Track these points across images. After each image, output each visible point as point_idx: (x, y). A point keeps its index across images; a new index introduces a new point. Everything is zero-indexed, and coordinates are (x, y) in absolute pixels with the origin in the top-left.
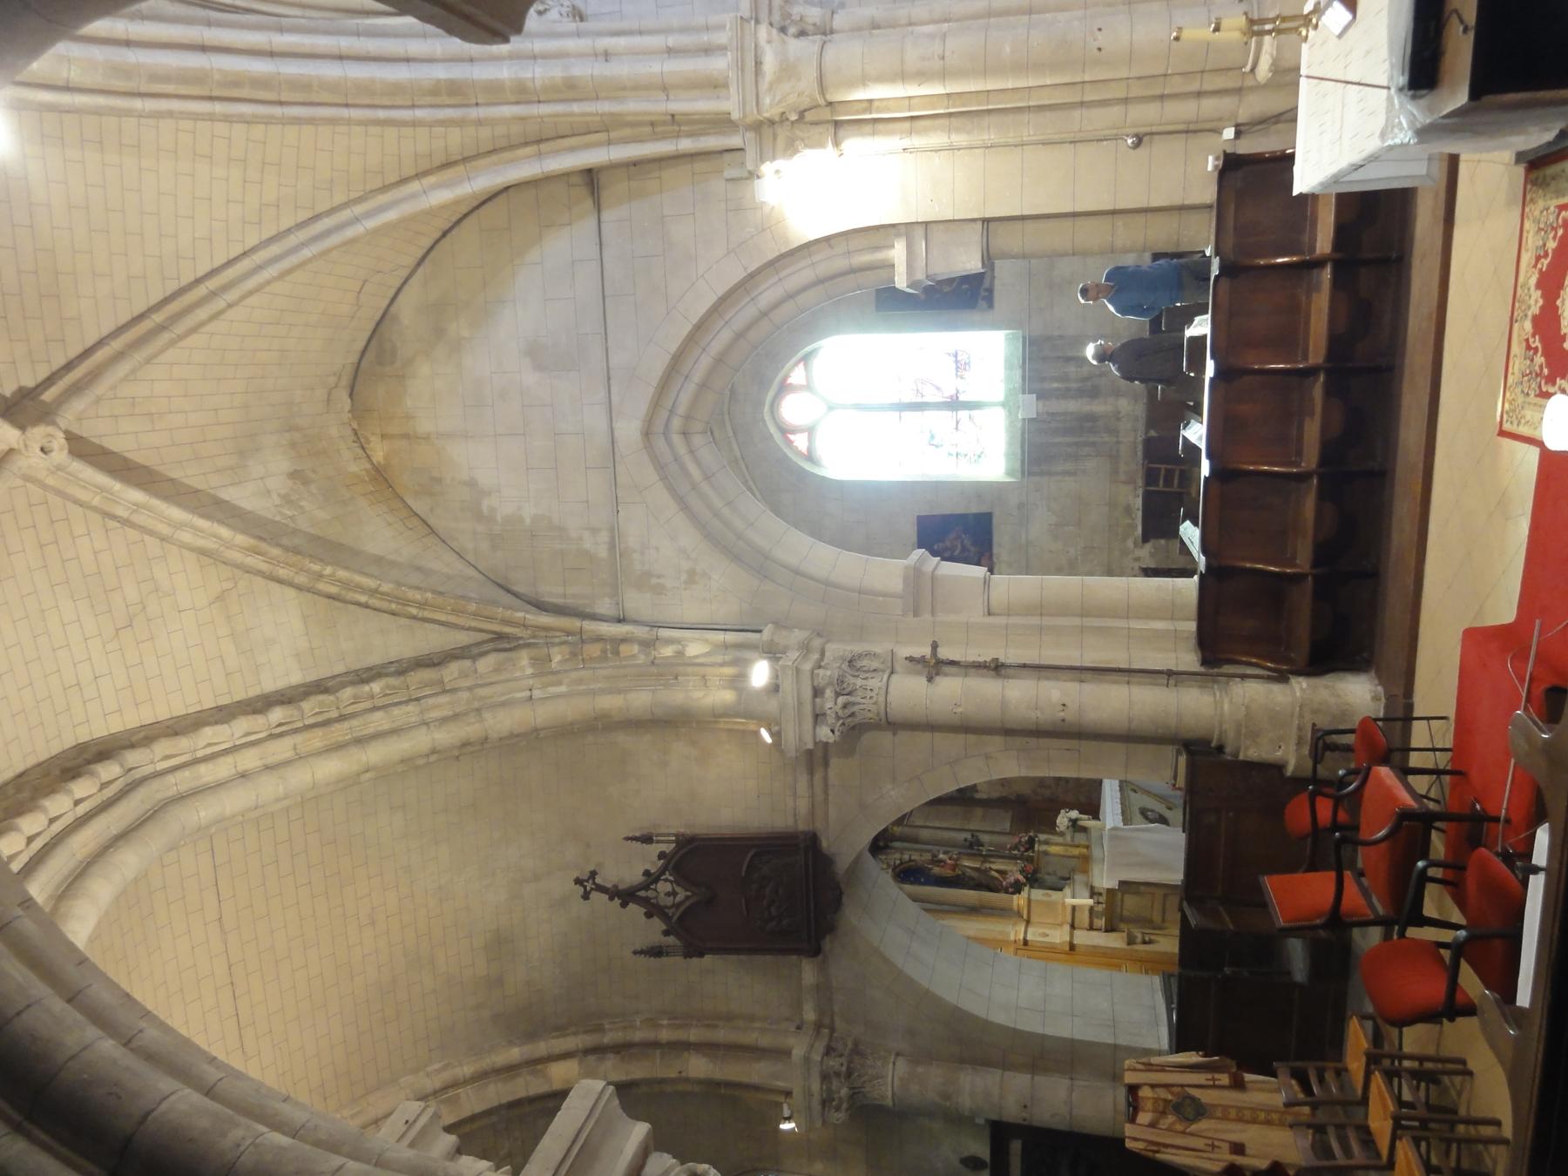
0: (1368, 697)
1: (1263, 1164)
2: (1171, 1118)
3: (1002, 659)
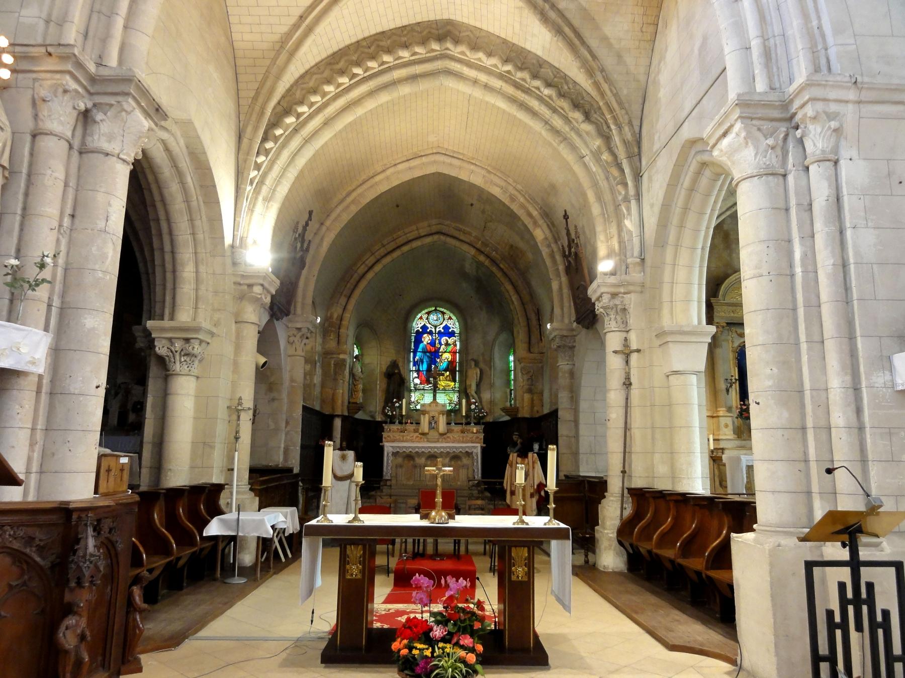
0: (606, 564)
3: (632, 387)
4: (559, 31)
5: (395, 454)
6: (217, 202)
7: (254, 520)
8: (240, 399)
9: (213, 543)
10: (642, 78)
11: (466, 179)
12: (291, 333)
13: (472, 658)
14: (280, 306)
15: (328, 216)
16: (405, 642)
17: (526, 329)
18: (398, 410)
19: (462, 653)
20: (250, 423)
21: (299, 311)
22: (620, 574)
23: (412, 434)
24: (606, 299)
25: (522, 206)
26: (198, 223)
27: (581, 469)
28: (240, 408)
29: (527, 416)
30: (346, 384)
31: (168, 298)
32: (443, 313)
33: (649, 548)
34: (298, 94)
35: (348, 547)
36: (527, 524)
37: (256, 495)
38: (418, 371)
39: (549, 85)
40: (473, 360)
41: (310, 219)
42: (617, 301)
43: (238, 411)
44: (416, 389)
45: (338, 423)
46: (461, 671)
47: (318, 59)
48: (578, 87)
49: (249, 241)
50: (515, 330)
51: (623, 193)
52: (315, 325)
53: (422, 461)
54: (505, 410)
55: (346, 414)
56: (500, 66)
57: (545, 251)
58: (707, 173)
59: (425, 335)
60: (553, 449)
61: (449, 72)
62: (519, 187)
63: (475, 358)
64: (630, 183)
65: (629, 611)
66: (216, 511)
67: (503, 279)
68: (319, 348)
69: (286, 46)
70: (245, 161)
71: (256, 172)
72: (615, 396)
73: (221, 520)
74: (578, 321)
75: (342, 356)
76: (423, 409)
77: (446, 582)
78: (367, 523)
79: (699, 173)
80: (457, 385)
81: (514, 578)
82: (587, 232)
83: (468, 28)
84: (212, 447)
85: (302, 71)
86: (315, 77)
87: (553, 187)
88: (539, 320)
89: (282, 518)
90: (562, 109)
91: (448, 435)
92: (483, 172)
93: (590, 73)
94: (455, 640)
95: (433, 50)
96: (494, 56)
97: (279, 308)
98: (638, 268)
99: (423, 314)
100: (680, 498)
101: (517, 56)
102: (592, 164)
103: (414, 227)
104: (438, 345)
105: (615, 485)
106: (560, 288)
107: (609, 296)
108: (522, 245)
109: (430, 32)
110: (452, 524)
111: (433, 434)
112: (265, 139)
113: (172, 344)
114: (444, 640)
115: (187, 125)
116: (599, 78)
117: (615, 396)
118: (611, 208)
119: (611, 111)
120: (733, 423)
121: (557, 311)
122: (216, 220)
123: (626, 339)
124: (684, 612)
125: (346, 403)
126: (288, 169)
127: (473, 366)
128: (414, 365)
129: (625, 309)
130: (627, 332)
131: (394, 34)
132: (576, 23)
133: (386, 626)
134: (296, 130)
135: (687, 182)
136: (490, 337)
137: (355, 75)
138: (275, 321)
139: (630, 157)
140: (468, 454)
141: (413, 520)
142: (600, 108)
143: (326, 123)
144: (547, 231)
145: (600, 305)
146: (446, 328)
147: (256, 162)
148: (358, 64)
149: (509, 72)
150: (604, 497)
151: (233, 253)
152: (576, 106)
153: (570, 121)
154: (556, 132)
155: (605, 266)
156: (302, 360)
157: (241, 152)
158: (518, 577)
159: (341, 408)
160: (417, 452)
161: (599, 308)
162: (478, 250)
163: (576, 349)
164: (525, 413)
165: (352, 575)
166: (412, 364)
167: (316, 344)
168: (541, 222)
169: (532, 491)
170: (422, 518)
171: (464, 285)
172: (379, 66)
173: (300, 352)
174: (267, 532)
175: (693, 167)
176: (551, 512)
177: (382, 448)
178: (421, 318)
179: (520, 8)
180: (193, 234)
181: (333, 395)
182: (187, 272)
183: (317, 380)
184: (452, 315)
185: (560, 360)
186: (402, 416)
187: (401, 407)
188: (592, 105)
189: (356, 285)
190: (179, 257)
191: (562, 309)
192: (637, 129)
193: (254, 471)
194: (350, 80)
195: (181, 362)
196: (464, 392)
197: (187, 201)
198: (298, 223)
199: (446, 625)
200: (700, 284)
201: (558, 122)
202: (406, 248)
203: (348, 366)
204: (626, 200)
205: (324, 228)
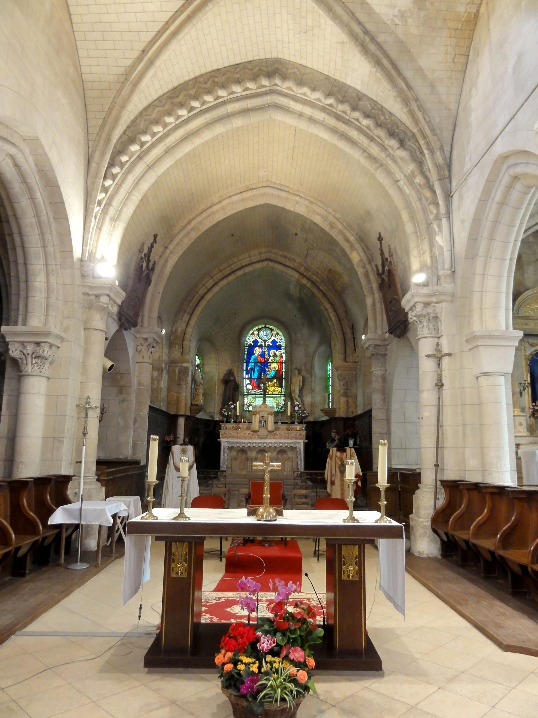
2: (340, 463)
3: (444, 388)
4: (378, 63)
5: (231, 448)
6: (66, 219)
7: (95, 510)
8: (88, 398)
9: (56, 531)
10: (453, 107)
11: (291, 209)
13: (302, 676)
14: (128, 317)
15: (172, 241)
16: (230, 654)
18: (233, 411)
19: (293, 670)
20: (97, 420)
21: (146, 323)
22: (435, 559)
24: (419, 308)
25: (341, 233)
26: (48, 237)
28: (87, 406)
30: (189, 388)
31: (21, 306)
32: (272, 330)
33: (466, 537)
34: (142, 125)
35: (173, 544)
36: (358, 521)
37: (102, 485)
38: (250, 378)
39: (367, 116)
40: (295, 368)
41: (155, 241)
42: (430, 310)
43: (86, 409)
44: (249, 394)
45: (181, 422)
46: (292, 691)
47: (160, 93)
48: (393, 118)
49: (98, 256)
50: (333, 344)
51: (435, 212)
52: (160, 336)
54: (325, 411)
55: (188, 413)
56: (323, 99)
57: (360, 272)
58: (519, 186)
59: (256, 348)
60: (385, 444)
61: (277, 107)
62: (338, 215)
63: (298, 367)
64: (441, 203)
65: (451, 601)
66: (63, 500)
67: (323, 300)
68: (165, 358)
69: (130, 79)
70: (94, 183)
71: (103, 195)
72: (428, 396)
73: (66, 510)
74: (391, 331)
75: (185, 365)
76: (255, 410)
77: (274, 584)
78: (193, 520)
79: (510, 187)
80: (283, 390)
81: (344, 577)
82: (399, 252)
83: (294, 65)
84: (61, 442)
85: (145, 104)
86: (157, 109)
87: (368, 213)
89: (124, 506)
90: (379, 138)
91: (276, 432)
92: (307, 203)
93: (406, 102)
94: (284, 653)
95: (263, 86)
96: (318, 90)
97: (127, 319)
98: (449, 280)
99: (254, 330)
100: (495, 490)
101: (338, 91)
102: (405, 188)
104: (267, 357)
105: (428, 478)
106: (374, 304)
107: (422, 305)
108: (339, 268)
109: (260, 70)
110: (280, 521)
111: (263, 431)
112: (111, 165)
113: (25, 347)
114: (273, 653)
115: (34, 142)
116: (414, 107)
117: (428, 396)
118: (423, 226)
119: (424, 137)
120: (527, 421)
121: (371, 323)
122: (65, 235)
123: (438, 344)
124: (507, 605)
125: (189, 405)
126: (133, 192)
127: (297, 374)
128: (247, 373)
129: (436, 317)
130: (439, 338)
131: (227, 71)
132: (393, 55)
133: (215, 620)
134: (140, 158)
135: (498, 196)
137: (192, 108)
138: (124, 331)
139: (441, 179)
140: (293, 449)
141: (238, 516)
142: (414, 135)
143: (168, 151)
144: (362, 254)
145: (414, 313)
146: (274, 342)
147: (103, 185)
148: (196, 98)
149: (331, 105)
150: (418, 488)
151: (82, 266)
152: (392, 134)
153: (386, 149)
154: (372, 158)
155: (418, 278)
156: (150, 367)
157: (89, 177)
158: (348, 576)
159: (184, 409)
161: (412, 317)
162: (301, 274)
163: (387, 357)
164: (341, 413)
165: (177, 573)
166: (245, 372)
167: (162, 353)
168: (357, 246)
170: (250, 514)
172: (215, 100)
173: (146, 359)
174: (108, 521)
175: (505, 180)
176: (383, 508)
178: (253, 334)
179: (343, 43)
180: (44, 247)
182: (39, 282)
183: (164, 384)
184: (279, 331)
185: (373, 366)
186: (236, 416)
187: (235, 408)
188: (406, 133)
189: (197, 305)
190: (30, 267)
191: (375, 322)
192: (448, 154)
193: (100, 463)
194: (189, 112)
195: (32, 364)
196: (289, 396)
197: (38, 216)
198: (143, 244)
199: (275, 634)
200: (507, 293)
201: (375, 150)
202: (240, 273)
203: (190, 373)
204: (438, 218)
205: (168, 252)
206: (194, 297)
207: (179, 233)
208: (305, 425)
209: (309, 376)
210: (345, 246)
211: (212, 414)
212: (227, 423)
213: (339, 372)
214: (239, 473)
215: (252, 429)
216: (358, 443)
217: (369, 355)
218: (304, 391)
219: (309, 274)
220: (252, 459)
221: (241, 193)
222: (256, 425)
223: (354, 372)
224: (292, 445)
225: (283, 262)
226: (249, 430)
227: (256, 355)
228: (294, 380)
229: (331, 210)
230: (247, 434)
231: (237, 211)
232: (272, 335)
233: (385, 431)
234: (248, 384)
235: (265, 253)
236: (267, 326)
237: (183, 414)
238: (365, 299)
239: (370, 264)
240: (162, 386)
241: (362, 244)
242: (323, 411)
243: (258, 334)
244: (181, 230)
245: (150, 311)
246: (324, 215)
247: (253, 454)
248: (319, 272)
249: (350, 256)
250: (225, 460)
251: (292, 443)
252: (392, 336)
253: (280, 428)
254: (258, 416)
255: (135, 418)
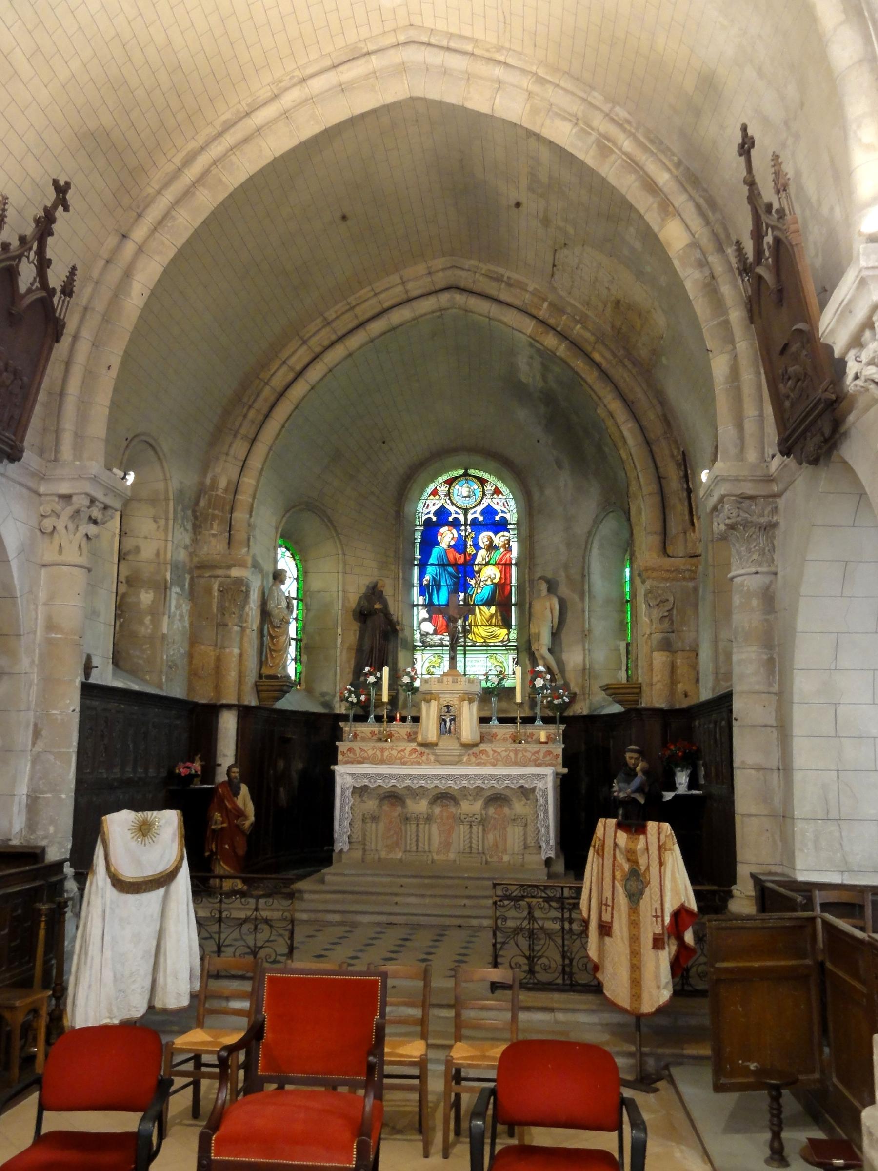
1: (592, 952)
2: (626, 867)
5: (360, 792)
12: (46, 509)
15: (139, 216)
17: (658, 498)
23: (402, 745)
25: (633, 165)
27: (799, 864)
29: (660, 703)
32: (482, 481)
38: (429, 606)
40: (540, 578)
44: (425, 645)
45: (228, 723)
53: (421, 806)
54: (613, 691)
55: (251, 700)
57: (691, 279)
59: (444, 530)
62: (621, 113)
63: (549, 575)
74: (787, 448)
75: (235, 573)
80: (513, 635)
87: (709, 85)
88: (686, 477)
91: (483, 746)
92: (525, 82)
103: (395, 278)
104: (471, 550)
108: (639, 294)
111: (448, 744)
121: (726, 431)
127: (544, 592)
128: (421, 593)
136: (581, 528)
140: (526, 793)
144: (696, 223)
160: (408, 788)
162: (543, 322)
163: (779, 532)
164: (655, 698)
166: (416, 590)
168: (680, 200)
169: (658, 930)
171: (522, 414)
173: (72, 555)
177: (333, 773)
178: (435, 493)
181: (218, 659)
184: (500, 485)
185: (735, 561)
186: (379, 703)
187: (378, 684)
191: (740, 426)
196: (526, 651)
205: (129, 248)
206: (258, 395)
207: (159, 192)
208: (562, 727)
209: (576, 597)
210: (643, 203)
211: (327, 698)
212: (357, 724)
213: (648, 583)
214: (383, 855)
215: (420, 739)
216: (702, 781)
217: (722, 527)
218: (563, 636)
219: (562, 322)
220: (417, 819)
221: (335, 67)
222: (429, 728)
223: (691, 584)
224: (522, 782)
225: (494, 293)
226: (414, 740)
227: (444, 545)
228: (537, 606)
229: (601, 98)
230: (407, 752)
231: (329, 125)
232: (484, 494)
233: (774, 761)
234: (425, 620)
235: (444, 269)
236: (471, 472)
237: (233, 701)
238: (709, 361)
239: (721, 250)
240: (165, 631)
241: (693, 193)
242: (606, 688)
243: (448, 494)
244: (167, 185)
245: (83, 418)
246: (580, 114)
247: (421, 806)
248: (590, 313)
249: (662, 236)
250: (346, 823)
251: (522, 776)
252: (790, 461)
253: (495, 735)
254: (434, 703)
255: (36, 725)
